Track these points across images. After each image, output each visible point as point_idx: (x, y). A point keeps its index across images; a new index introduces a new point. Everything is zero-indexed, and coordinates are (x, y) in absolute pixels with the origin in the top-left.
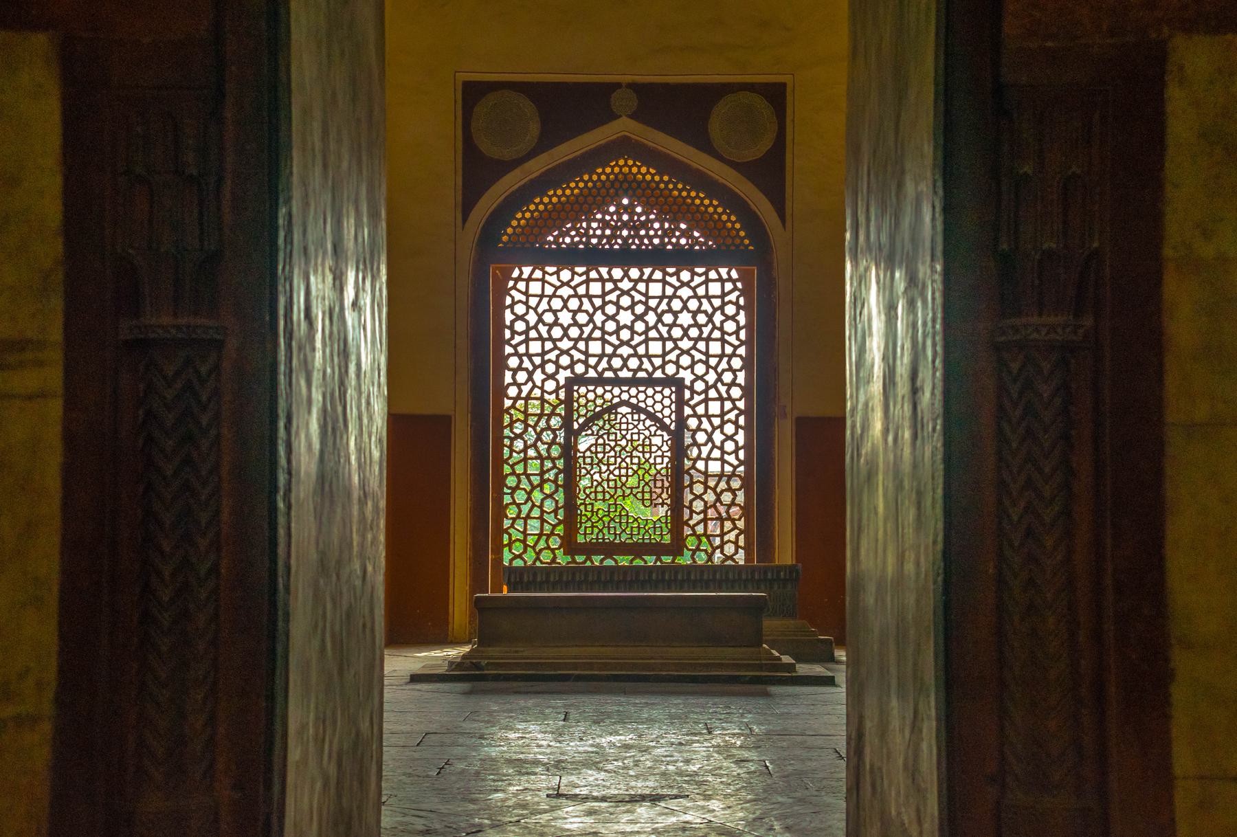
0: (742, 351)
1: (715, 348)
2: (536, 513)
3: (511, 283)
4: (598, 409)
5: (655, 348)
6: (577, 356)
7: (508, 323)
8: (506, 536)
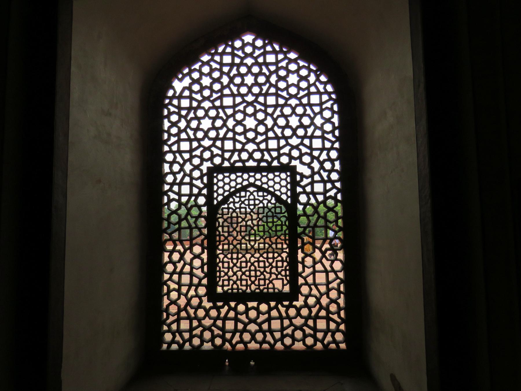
0: (337, 145)
1: (317, 143)
2: (187, 268)
3: (167, 101)
4: (232, 190)
5: (273, 144)
6: (216, 151)
7: (166, 129)
8: (165, 288)
